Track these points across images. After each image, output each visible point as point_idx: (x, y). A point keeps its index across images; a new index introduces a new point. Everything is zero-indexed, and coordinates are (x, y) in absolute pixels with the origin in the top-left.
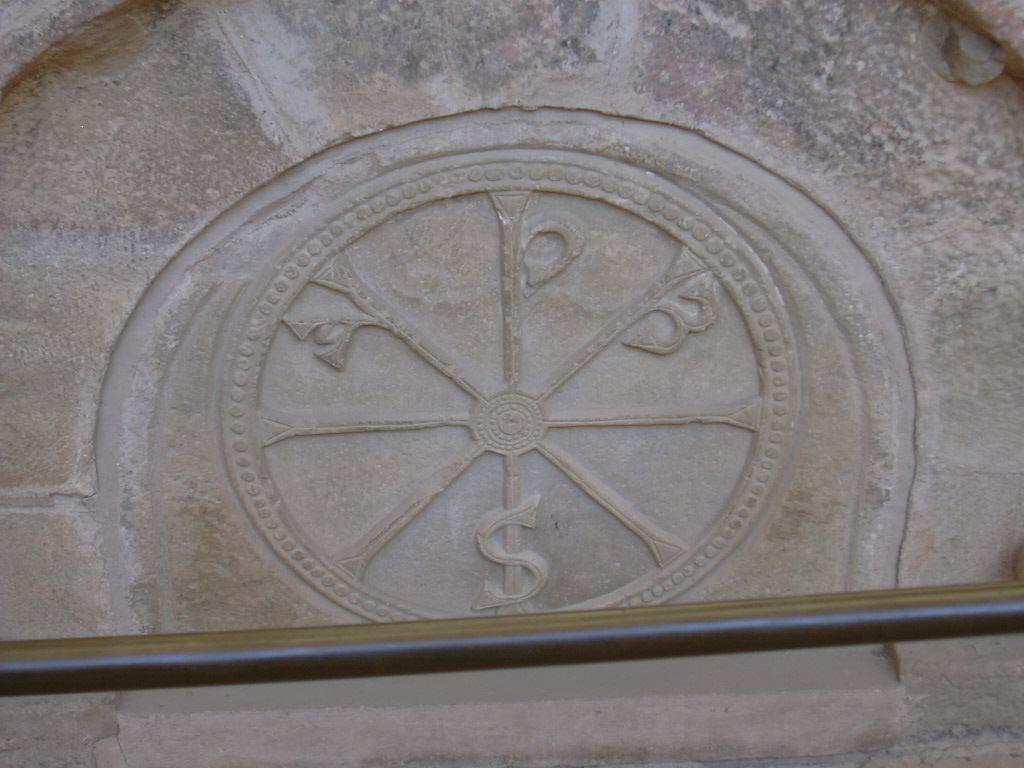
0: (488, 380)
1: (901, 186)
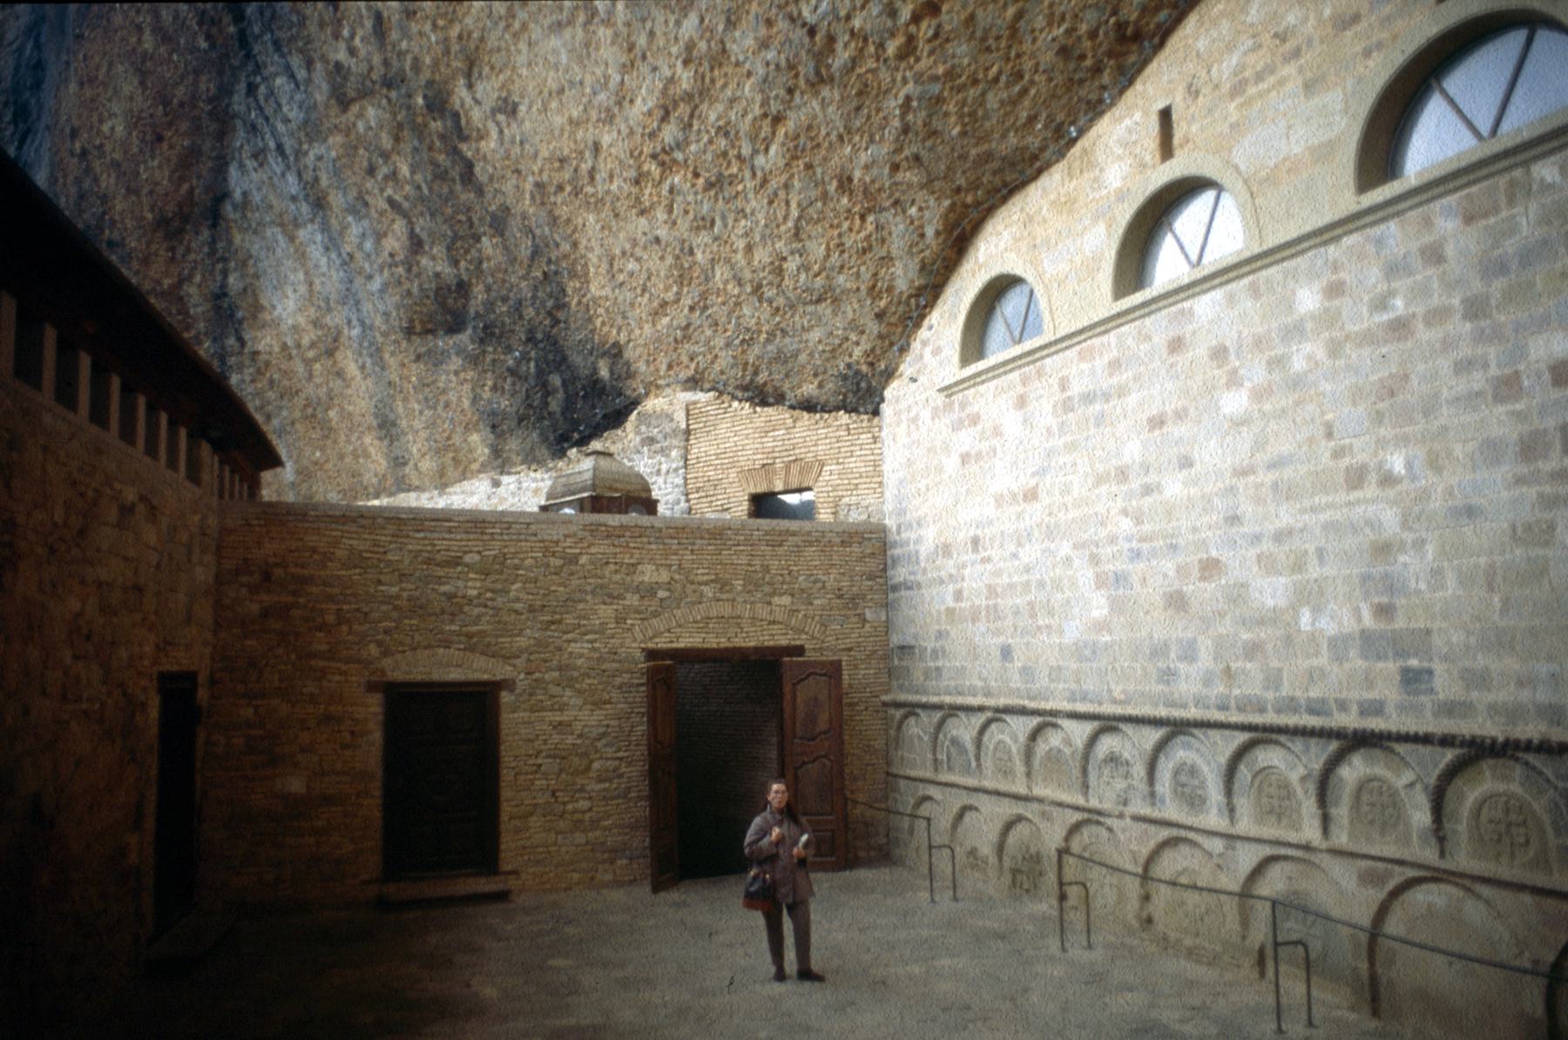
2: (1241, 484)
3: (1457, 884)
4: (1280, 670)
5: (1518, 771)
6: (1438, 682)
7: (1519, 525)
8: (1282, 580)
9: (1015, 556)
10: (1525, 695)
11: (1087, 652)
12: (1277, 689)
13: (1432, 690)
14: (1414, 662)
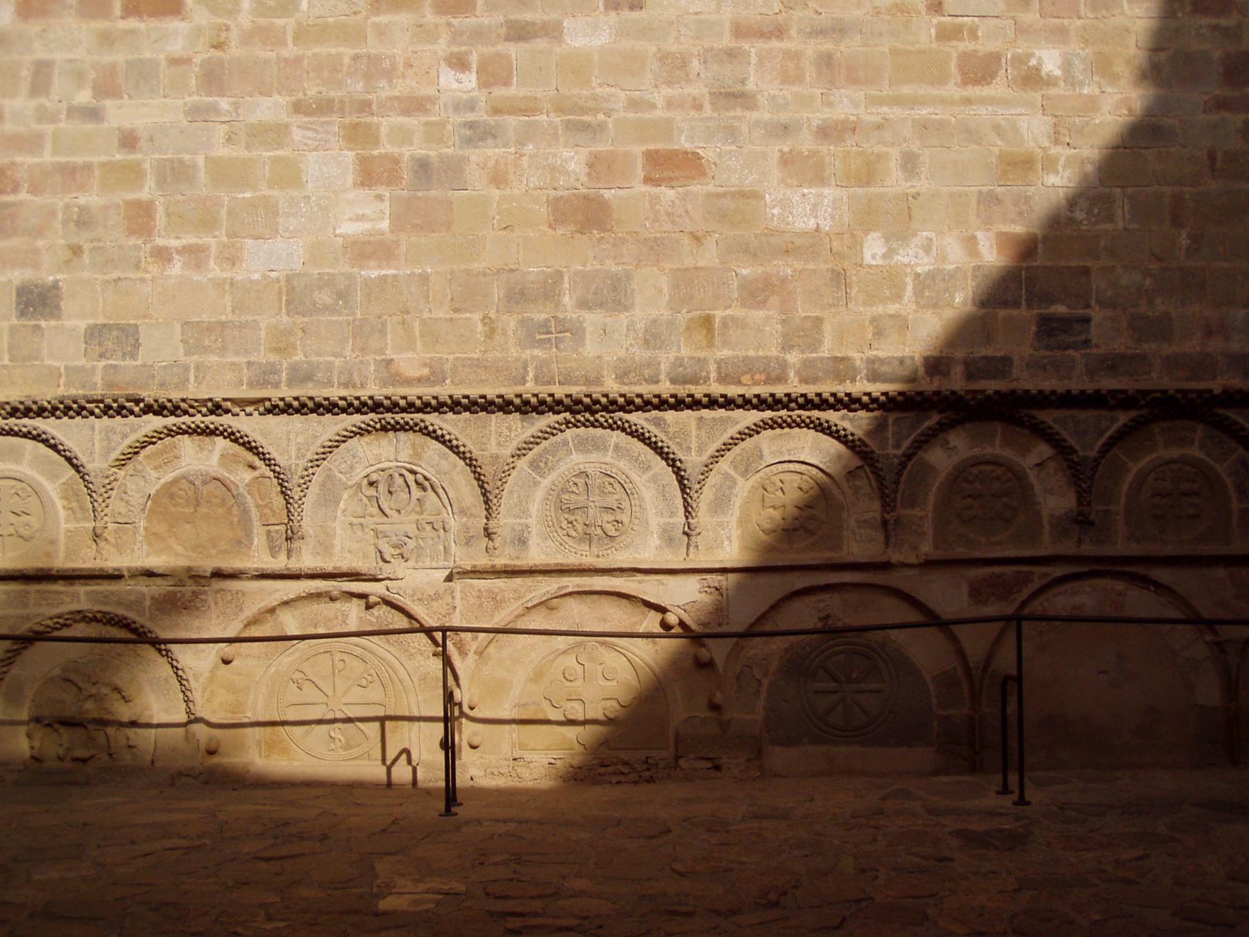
0: (330, 693)
1: (407, 651)
2: (753, 48)
3: (1119, 575)
4: (818, 322)
5: (1200, 431)
6: (1094, 334)
7: (1219, 155)
8: (829, 192)
9: (93, 114)
10: (1215, 345)
11: (324, 297)
12: (815, 345)
13: (1087, 342)
14: (1060, 309)
